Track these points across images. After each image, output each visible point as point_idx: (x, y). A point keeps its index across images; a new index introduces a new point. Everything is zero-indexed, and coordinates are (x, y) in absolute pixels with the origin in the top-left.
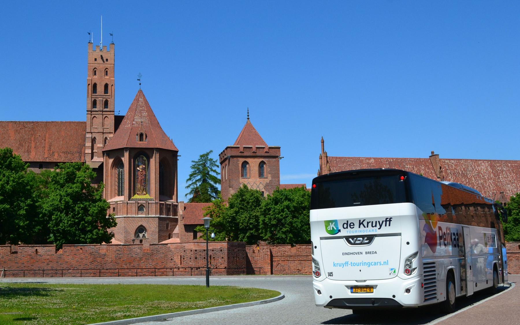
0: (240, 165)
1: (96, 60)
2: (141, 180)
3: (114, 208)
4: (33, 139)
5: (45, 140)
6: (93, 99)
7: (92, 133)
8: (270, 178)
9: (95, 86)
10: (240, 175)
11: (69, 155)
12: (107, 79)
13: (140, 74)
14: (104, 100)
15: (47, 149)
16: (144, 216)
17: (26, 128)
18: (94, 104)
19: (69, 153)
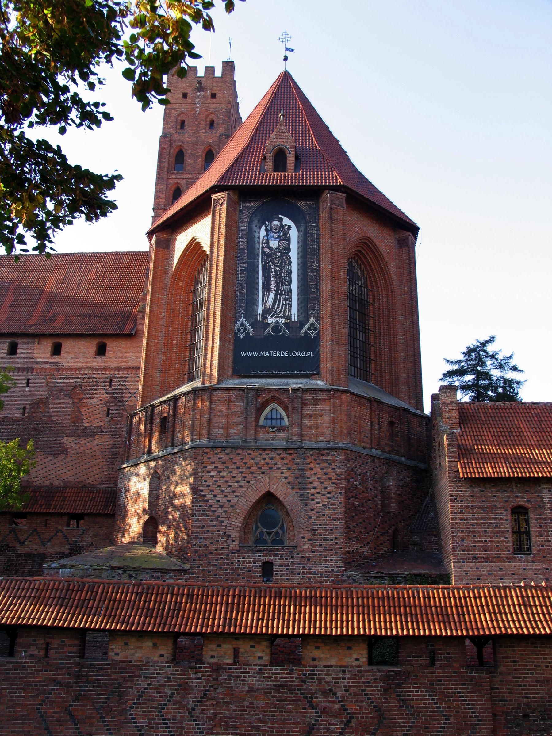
3: (164, 420)
13: (285, 34)
16: (284, 444)
19: (96, 316)
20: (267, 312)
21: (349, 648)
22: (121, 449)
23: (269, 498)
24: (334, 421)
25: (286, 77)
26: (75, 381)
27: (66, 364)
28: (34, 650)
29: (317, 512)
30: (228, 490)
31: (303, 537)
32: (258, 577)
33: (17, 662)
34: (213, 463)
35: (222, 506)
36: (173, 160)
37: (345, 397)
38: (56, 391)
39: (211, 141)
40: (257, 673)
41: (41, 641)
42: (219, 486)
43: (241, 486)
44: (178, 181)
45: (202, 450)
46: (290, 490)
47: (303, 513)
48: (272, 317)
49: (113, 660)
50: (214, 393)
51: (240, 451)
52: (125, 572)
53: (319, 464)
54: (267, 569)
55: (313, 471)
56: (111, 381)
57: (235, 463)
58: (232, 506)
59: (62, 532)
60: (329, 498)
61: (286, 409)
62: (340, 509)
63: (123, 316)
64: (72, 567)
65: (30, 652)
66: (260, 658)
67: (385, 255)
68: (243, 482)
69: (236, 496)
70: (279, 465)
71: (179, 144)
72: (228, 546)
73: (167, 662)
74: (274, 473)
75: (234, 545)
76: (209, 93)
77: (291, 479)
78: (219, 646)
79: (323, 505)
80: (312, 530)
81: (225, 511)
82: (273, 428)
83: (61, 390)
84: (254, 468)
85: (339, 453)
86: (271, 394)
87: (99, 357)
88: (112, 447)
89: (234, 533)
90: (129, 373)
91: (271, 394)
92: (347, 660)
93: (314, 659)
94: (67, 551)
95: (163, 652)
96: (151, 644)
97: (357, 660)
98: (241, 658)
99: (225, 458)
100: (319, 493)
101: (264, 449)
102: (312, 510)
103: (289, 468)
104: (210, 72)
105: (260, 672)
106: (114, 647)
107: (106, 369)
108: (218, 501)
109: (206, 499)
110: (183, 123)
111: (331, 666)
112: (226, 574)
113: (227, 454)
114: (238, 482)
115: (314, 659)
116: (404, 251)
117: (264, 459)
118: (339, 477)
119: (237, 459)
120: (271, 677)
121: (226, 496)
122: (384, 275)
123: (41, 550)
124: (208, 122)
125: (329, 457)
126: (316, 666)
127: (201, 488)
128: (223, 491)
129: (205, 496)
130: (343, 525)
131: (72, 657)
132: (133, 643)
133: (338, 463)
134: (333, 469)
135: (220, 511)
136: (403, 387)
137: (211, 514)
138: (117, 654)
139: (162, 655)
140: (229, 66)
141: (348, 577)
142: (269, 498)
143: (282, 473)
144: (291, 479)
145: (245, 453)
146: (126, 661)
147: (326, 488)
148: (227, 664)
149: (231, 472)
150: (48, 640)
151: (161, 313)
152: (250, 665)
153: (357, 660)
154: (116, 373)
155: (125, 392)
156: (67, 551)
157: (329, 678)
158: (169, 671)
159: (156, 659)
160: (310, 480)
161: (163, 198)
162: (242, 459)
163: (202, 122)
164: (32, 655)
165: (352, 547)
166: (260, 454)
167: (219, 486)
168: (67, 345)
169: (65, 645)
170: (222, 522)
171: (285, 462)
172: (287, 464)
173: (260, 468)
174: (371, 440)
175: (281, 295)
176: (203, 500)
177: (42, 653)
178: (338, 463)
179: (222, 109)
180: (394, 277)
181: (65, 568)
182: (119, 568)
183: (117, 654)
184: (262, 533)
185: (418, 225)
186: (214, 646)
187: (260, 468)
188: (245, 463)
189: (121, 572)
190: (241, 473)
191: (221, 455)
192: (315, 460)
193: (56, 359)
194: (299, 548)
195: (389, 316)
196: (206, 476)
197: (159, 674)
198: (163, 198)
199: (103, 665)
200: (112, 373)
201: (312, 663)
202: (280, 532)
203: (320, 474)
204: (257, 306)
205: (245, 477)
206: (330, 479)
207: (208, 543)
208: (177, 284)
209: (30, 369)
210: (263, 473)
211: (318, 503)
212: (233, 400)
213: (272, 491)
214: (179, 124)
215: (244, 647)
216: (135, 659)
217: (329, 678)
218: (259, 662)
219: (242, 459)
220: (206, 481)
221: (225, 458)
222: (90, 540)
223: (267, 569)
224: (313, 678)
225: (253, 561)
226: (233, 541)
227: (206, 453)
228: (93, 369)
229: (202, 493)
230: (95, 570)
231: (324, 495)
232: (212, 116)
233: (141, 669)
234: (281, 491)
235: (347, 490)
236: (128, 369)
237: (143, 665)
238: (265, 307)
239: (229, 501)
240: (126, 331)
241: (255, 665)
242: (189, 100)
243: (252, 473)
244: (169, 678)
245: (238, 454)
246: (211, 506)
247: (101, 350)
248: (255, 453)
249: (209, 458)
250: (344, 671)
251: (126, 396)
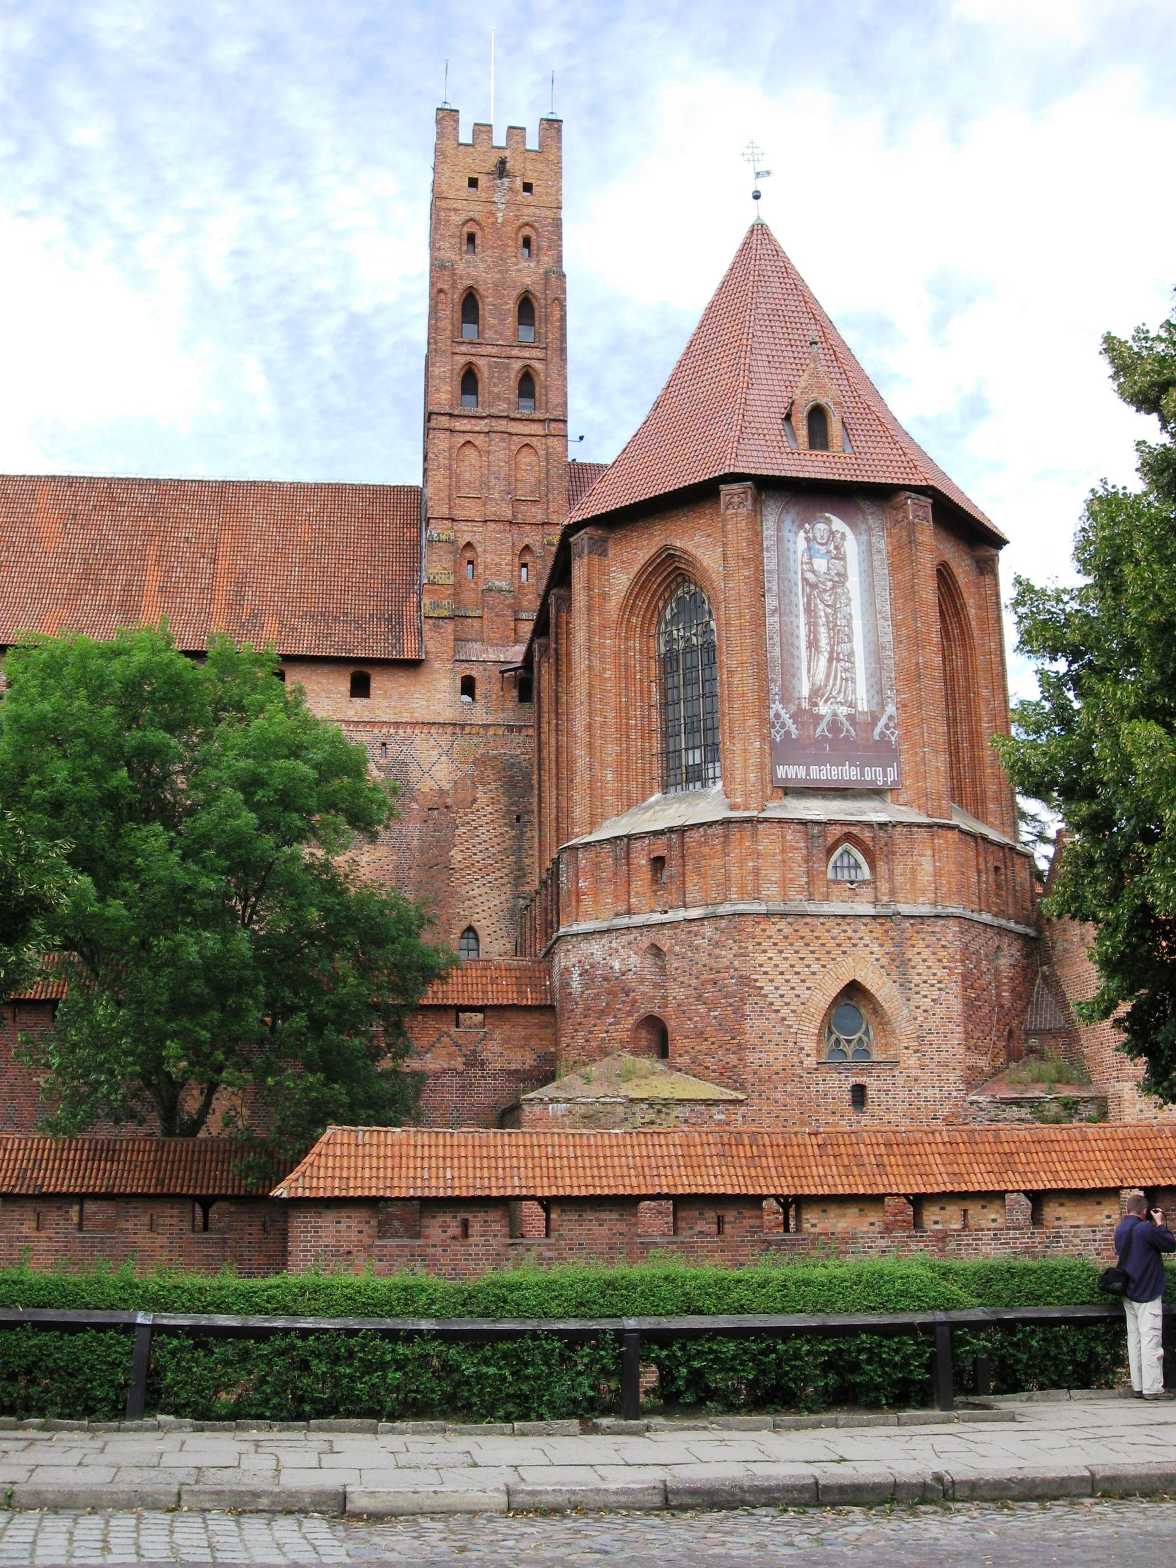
1: (473, 183)
3: (658, 863)
4: (152, 552)
5: (214, 561)
6: (462, 360)
7: (453, 520)
9: (470, 306)
11: (338, 628)
12: (526, 273)
13: (752, 145)
14: (517, 365)
15: (221, 597)
16: (869, 910)
17: (122, 504)
18: (469, 381)
19: (336, 619)
20: (816, 692)
21: (1099, 1203)
22: (412, 872)
23: (854, 991)
24: (937, 874)
25: (759, 231)
28: (701, 1226)
29: (925, 1011)
30: (795, 980)
31: (907, 1048)
32: (846, 1105)
33: (682, 1242)
34: (770, 937)
35: (787, 1004)
36: (458, 315)
37: (952, 836)
39: (528, 281)
40: (992, 1239)
41: (711, 1215)
42: (782, 973)
43: (814, 973)
44: (473, 359)
45: (751, 918)
46: (885, 978)
47: (905, 1012)
48: (826, 702)
49: (810, 1234)
50: (759, 826)
51: (808, 920)
52: (651, 1105)
53: (923, 939)
54: (859, 1094)
55: (916, 950)
56: (384, 744)
57: (802, 938)
58: (803, 1004)
59: (449, 1036)
60: (940, 989)
61: (866, 852)
62: (957, 1005)
63: (389, 620)
64: (568, 1101)
65: (698, 1228)
66: (994, 1220)
67: (963, 589)
68: (815, 967)
69: (808, 988)
70: (867, 940)
71: (469, 283)
72: (801, 1062)
73: (880, 1233)
74: (860, 951)
75: (810, 1062)
76: (519, 183)
77: (884, 961)
78: (943, 1208)
79: (933, 1000)
80: (918, 1037)
81: (793, 1011)
82: (852, 882)
84: (831, 944)
85: (951, 922)
86: (846, 829)
87: (357, 700)
88: (396, 868)
89: (809, 1044)
90: (417, 732)
91: (846, 829)
92: (1099, 1217)
93: (1058, 1219)
94: (461, 1068)
95: (872, 1220)
96: (856, 1210)
97: (1108, 1217)
98: (971, 1222)
99: (787, 930)
100: (925, 982)
101: (844, 916)
102: (918, 1007)
103: (881, 946)
104: (518, 138)
105: (996, 1238)
106: (808, 1216)
107: (372, 723)
108: (782, 996)
109: (763, 992)
110: (471, 238)
111: (1078, 1227)
112: (801, 1104)
113: (790, 924)
114: (808, 966)
115: (1058, 1219)
116: (988, 580)
117: (845, 931)
118: (952, 958)
119: (805, 931)
120: (1008, 1243)
121: (793, 988)
122: (959, 621)
124: (520, 242)
125: (937, 929)
126: (1061, 1227)
127: (755, 977)
128: (788, 981)
129: (761, 988)
130: (960, 1029)
131: (755, 1232)
132: (833, 1212)
133: (950, 937)
134: (943, 946)
135: (785, 1011)
136: (991, 806)
137: (773, 1015)
138: (814, 1225)
139: (872, 1224)
140: (552, 126)
141: (972, 1103)
142: (854, 991)
143: (872, 953)
144: (884, 961)
145: (815, 921)
146: (826, 1234)
147: (935, 974)
148: (955, 1230)
149: (797, 952)
150: (720, 1213)
151: (605, 670)
152: (983, 1230)
153: (1108, 1217)
154: (392, 731)
155: (413, 767)
156: (461, 1068)
157: (1077, 1241)
158: (882, 1243)
159: (865, 1229)
160: (912, 964)
161: (446, 392)
162: (812, 931)
163: (510, 243)
164: (701, 1232)
165: (970, 1061)
166: (838, 924)
167: (782, 973)
169: (745, 1218)
170: (790, 1027)
171: (874, 935)
172: (877, 939)
173: (839, 945)
174: (980, 899)
175: (838, 660)
176: (759, 995)
177: (714, 1228)
178: (950, 937)
179: (545, 218)
180: (973, 623)
181: (558, 1102)
182: (642, 1100)
183: (814, 1225)
184: (838, 1041)
185: (1007, 536)
186: (936, 1209)
187: (839, 945)
188: (818, 938)
189: (644, 1106)
190: (813, 952)
191: (782, 924)
192: (917, 932)
194: (902, 1065)
195: (968, 689)
196: (762, 958)
197: (870, 1247)
198: (446, 392)
199: (797, 1240)
200: (384, 730)
201: (1057, 1223)
202: (865, 1039)
203: (926, 953)
204: (800, 679)
205: (818, 959)
206: (940, 961)
207: (772, 1059)
208: (629, 621)
210: (844, 953)
211: (925, 997)
212: (789, 838)
213: (859, 980)
214: (465, 241)
215: (974, 1209)
216: (839, 1230)
217: (1077, 1241)
218: (993, 1225)
219: (812, 931)
220: (761, 966)
221: (787, 930)
222: (497, 1049)
223: (859, 1094)
224: (1058, 1242)
225: (840, 1084)
226: (808, 1055)
227: (758, 923)
228: (348, 723)
229: (758, 984)
230: (604, 1104)
231: (933, 985)
232: (527, 231)
233: (847, 1243)
234: (872, 980)
235: (965, 977)
236: (414, 724)
237: (851, 1238)
238: (813, 684)
239: (798, 996)
240: (408, 655)
241: (989, 1230)
242: (480, 193)
243: (828, 953)
244: (884, 1252)
245: (807, 924)
246: (772, 1004)
247: (360, 687)
248: (831, 923)
249: (764, 930)
250: (1094, 1231)
251: (414, 774)
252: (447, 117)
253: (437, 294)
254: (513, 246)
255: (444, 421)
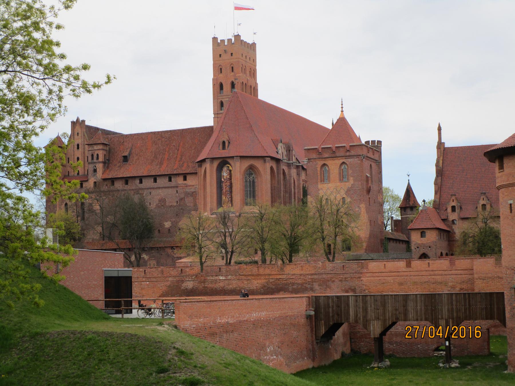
0: (319, 169)
1: (220, 55)
2: (226, 192)
4: (167, 149)
5: (178, 150)
8: (351, 181)
9: (221, 86)
10: (319, 180)
15: (178, 159)
26: (193, 190)
27: (189, 184)
38: (187, 194)
83: (189, 194)
123: (180, 256)
168: (188, 177)
193: (185, 182)
209: (177, 187)
252: (215, 39)
253: (214, 85)
254: (229, 70)
255: (216, 116)
